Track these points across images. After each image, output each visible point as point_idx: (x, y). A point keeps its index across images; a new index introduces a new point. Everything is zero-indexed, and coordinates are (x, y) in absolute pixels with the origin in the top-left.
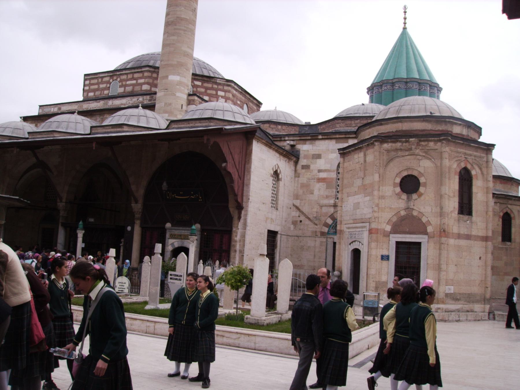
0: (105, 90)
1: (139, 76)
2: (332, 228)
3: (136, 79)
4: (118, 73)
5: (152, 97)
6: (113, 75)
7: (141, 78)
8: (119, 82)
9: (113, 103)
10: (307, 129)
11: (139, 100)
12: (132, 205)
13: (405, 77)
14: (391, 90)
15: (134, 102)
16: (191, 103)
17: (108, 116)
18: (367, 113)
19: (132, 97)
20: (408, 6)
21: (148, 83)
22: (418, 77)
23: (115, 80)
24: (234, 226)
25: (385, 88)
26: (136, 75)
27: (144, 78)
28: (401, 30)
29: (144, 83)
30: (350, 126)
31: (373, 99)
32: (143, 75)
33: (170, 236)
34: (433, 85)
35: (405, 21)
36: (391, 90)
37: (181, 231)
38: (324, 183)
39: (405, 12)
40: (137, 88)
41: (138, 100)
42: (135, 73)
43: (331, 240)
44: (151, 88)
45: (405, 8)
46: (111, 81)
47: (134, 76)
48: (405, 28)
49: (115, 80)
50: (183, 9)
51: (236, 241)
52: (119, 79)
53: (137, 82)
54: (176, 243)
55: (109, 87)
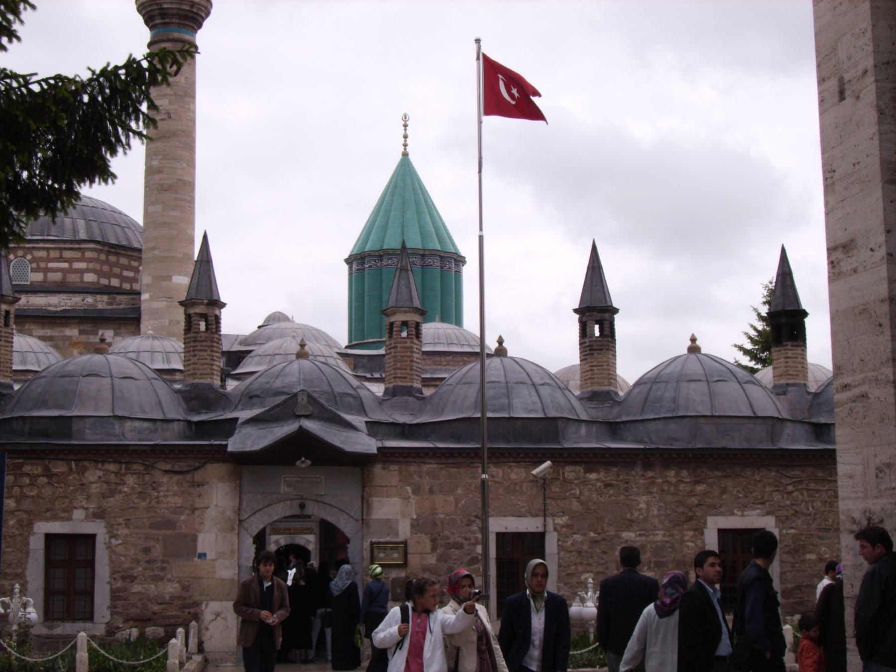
3: (70, 261)
5: (114, 298)
6: (14, 247)
8: (31, 262)
9: (28, 302)
10: (365, 361)
11: (85, 301)
13: (420, 247)
15: (76, 303)
17: (33, 327)
18: (452, 344)
19: (71, 295)
20: (410, 115)
21: (93, 271)
22: (439, 249)
23: (20, 257)
25: (390, 261)
26: (67, 254)
27: (85, 262)
28: (400, 157)
29: (87, 270)
30: (439, 365)
31: (364, 278)
32: (83, 255)
34: (458, 259)
35: (405, 141)
37: (289, 524)
39: (405, 126)
40: (73, 278)
41: (83, 300)
42: (66, 249)
45: (405, 118)
47: (63, 254)
48: (405, 155)
49: (20, 257)
50: (185, 165)
52: (29, 257)
53: (71, 266)
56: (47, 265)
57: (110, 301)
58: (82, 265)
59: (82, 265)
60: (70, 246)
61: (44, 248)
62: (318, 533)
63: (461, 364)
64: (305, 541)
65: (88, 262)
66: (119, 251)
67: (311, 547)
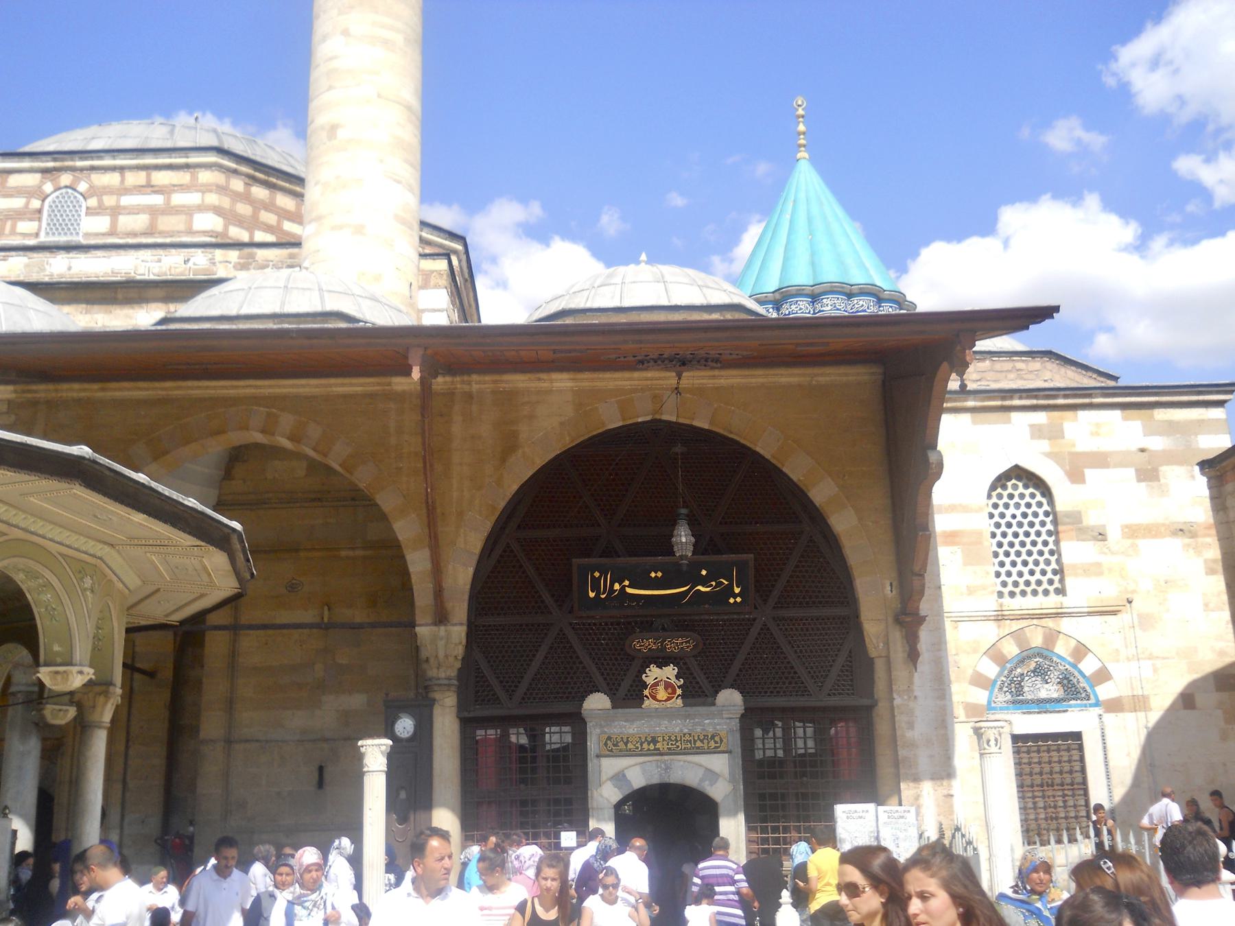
0: (21, 219)
1: (175, 182)
2: (1001, 689)
4: (79, 164)
5: (252, 256)
7: (182, 188)
9: (70, 268)
11: (190, 264)
12: (418, 629)
14: (809, 313)
16: (432, 283)
21: (218, 211)
24: (899, 685)
26: (161, 178)
29: (201, 208)
32: (194, 178)
33: (606, 744)
36: (809, 313)
38: (955, 548)
40: (169, 223)
41: (186, 262)
43: (1007, 730)
44: (226, 227)
46: (48, 187)
49: (66, 187)
51: (912, 745)
53: (168, 200)
54: (638, 768)
55: (40, 211)
56: (118, 201)
57: (242, 261)
58: (193, 198)
59: (193, 198)
60: (167, 161)
61: (113, 169)
62: (739, 750)
63: (1012, 376)
64: (701, 772)
65: (203, 192)
66: (274, 180)
67: (719, 791)
